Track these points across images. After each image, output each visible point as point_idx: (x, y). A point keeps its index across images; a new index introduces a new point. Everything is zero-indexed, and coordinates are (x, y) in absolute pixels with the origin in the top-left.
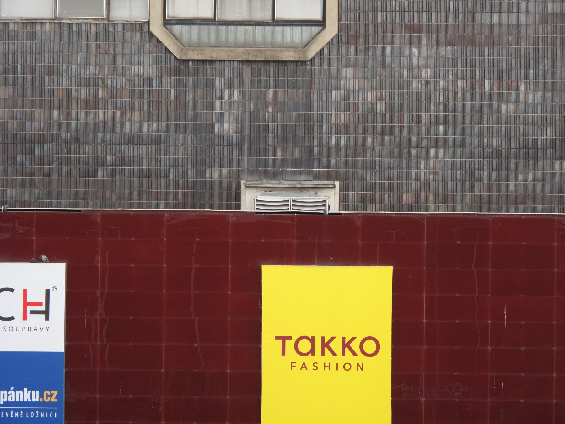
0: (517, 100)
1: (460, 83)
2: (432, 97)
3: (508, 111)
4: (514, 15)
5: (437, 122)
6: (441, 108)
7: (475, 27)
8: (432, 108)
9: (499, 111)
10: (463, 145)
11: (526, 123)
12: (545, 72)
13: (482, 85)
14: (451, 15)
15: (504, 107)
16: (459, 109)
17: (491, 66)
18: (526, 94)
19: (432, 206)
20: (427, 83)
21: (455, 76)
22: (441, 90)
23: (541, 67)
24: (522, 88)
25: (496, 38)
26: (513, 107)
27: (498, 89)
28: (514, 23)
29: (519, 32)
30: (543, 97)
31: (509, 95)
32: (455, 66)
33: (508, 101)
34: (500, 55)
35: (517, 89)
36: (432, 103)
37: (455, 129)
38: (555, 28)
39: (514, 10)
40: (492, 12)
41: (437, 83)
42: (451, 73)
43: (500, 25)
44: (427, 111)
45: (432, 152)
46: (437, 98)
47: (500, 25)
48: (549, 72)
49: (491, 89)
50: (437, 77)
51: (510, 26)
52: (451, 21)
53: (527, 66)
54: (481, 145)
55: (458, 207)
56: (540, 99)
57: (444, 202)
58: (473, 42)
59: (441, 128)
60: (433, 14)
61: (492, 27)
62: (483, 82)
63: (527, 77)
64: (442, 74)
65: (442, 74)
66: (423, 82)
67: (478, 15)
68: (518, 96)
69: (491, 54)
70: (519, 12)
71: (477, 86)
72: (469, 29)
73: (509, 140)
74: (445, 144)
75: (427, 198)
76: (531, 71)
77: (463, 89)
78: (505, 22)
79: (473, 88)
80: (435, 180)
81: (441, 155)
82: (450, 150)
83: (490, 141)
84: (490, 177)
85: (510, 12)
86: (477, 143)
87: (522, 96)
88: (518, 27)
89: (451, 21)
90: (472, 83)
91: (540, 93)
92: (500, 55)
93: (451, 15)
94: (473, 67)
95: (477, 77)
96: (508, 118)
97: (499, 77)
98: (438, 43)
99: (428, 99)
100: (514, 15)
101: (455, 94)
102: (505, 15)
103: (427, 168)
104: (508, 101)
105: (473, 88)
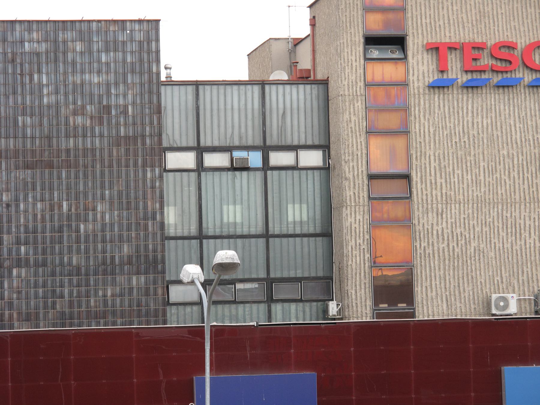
0: (95, 220)
1: (39, 205)
2: (13, 220)
3: (86, 231)
4: (89, 140)
5: (18, 243)
6: (22, 229)
7: (52, 151)
8: (14, 230)
9: (78, 231)
10: (44, 264)
11: (104, 241)
12: (120, 193)
13: (60, 206)
14: (29, 140)
15: (82, 226)
16: (39, 230)
17: (68, 188)
18: (103, 213)
19: (16, 324)
20: (8, 206)
21: (34, 198)
22: (21, 213)
23: (116, 188)
24: (99, 209)
25: (72, 162)
26: (91, 227)
27: (76, 210)
28: (89, 146)
29: (94, 155)
30: (119, 216)
31: (86, 215)
32: (34, 189)
33: (86, 221)
34: (77, 177)
35: (94, 209)
36: (13, 225)
37: (36, 249)
38: (127, 151)
39: (89, 135)
40: (67, 136)
41: (17, 206)
42: (30, 195)
43: (76, 149)
44: (9, 232)
45: (15, 272)
46: (18, 220)
47: (76, 149)
48: (124, 193)
49: (70, 210)
50: (17, 200)
51: (85, 150)
52: (29, 146)
53: (103, 187)
54: (62, 264)
55: (42, 324)
56: (116, 218)
57: (28, 319)
58: (50, 166)
59: (23, 248)
60: (12, 140)
61: (68, 151)
62: (61, 204)
63: (103, 198)
64: (21, 197)
65: (21, 197)
66: (4, 205)
67: (55, 140)
68: (95, 216)
69: (68, 177)
70: (93, 136)
71: (56, 208)
72: (47, 153)
73: (87, 258)
74: (27, 264)
75: (11, 317)
76: (107, 192)
77: (42, 211)
78: (80, 146)
79: (52, 209)
80: (18, 299)
81: (23, 275)
82: (32, 270)
83: (70, 259)
84: (71, 294)
85: (84, 136)
86: (57, 261)
87: (99, 216)
88: (93, 150)
89: (29, 146)
90: (50, 204)
91: (116, 212)
92: (77, 177)
93: (29, 140)
94: (51, 189)
95: (56, 199)
96: (87, 236)
97: (77, 198)
98: (17, 168)
99: (9, 221)
100: (89, 140)
101: (35, 216)
102: (80, 139)
103: (10, 287)
104: (86, 221)
105: (52, 209)
